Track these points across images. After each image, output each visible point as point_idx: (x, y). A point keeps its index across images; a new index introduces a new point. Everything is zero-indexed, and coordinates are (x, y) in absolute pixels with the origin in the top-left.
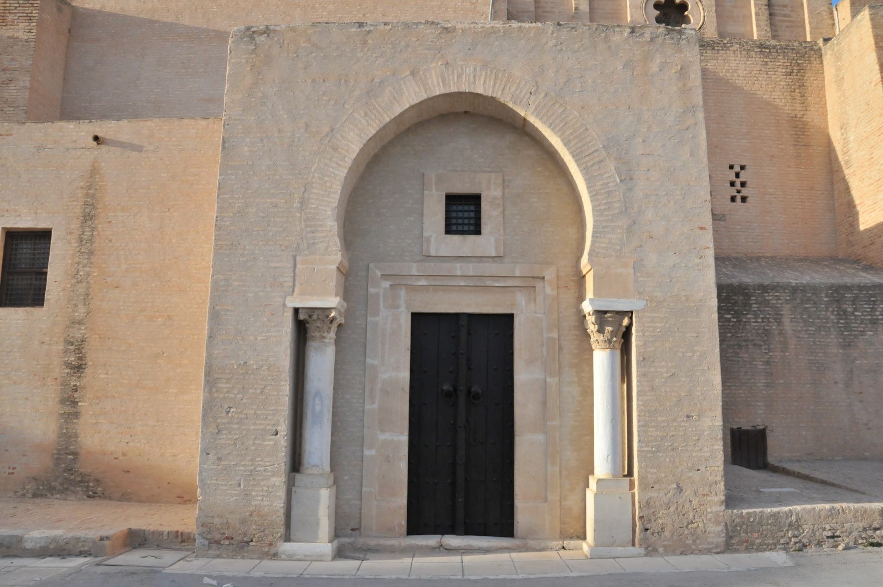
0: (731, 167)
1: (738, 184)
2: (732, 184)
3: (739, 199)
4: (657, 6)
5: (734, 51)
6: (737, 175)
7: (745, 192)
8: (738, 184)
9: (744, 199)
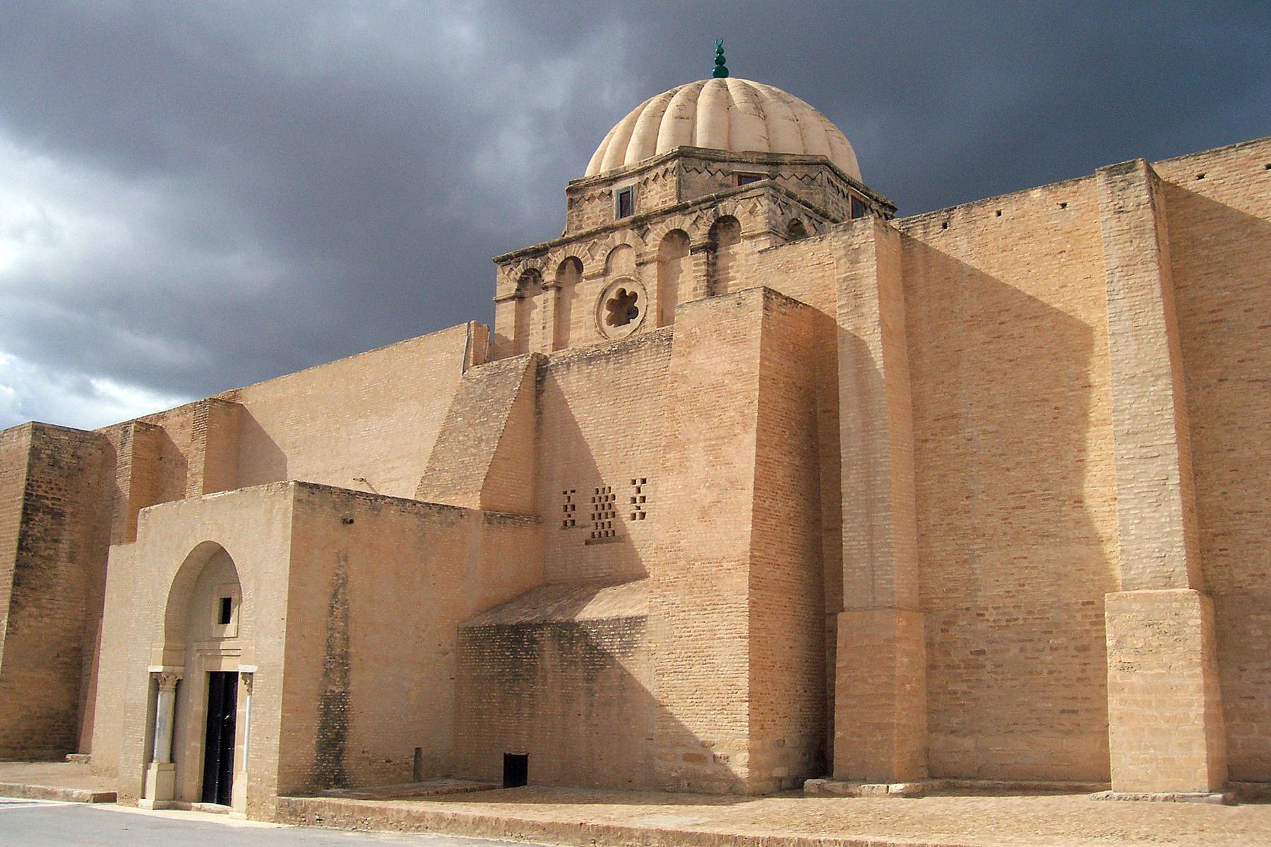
0: (634, 482)
2: (634, 500)
6: (639, 491)
9: (643, 515)
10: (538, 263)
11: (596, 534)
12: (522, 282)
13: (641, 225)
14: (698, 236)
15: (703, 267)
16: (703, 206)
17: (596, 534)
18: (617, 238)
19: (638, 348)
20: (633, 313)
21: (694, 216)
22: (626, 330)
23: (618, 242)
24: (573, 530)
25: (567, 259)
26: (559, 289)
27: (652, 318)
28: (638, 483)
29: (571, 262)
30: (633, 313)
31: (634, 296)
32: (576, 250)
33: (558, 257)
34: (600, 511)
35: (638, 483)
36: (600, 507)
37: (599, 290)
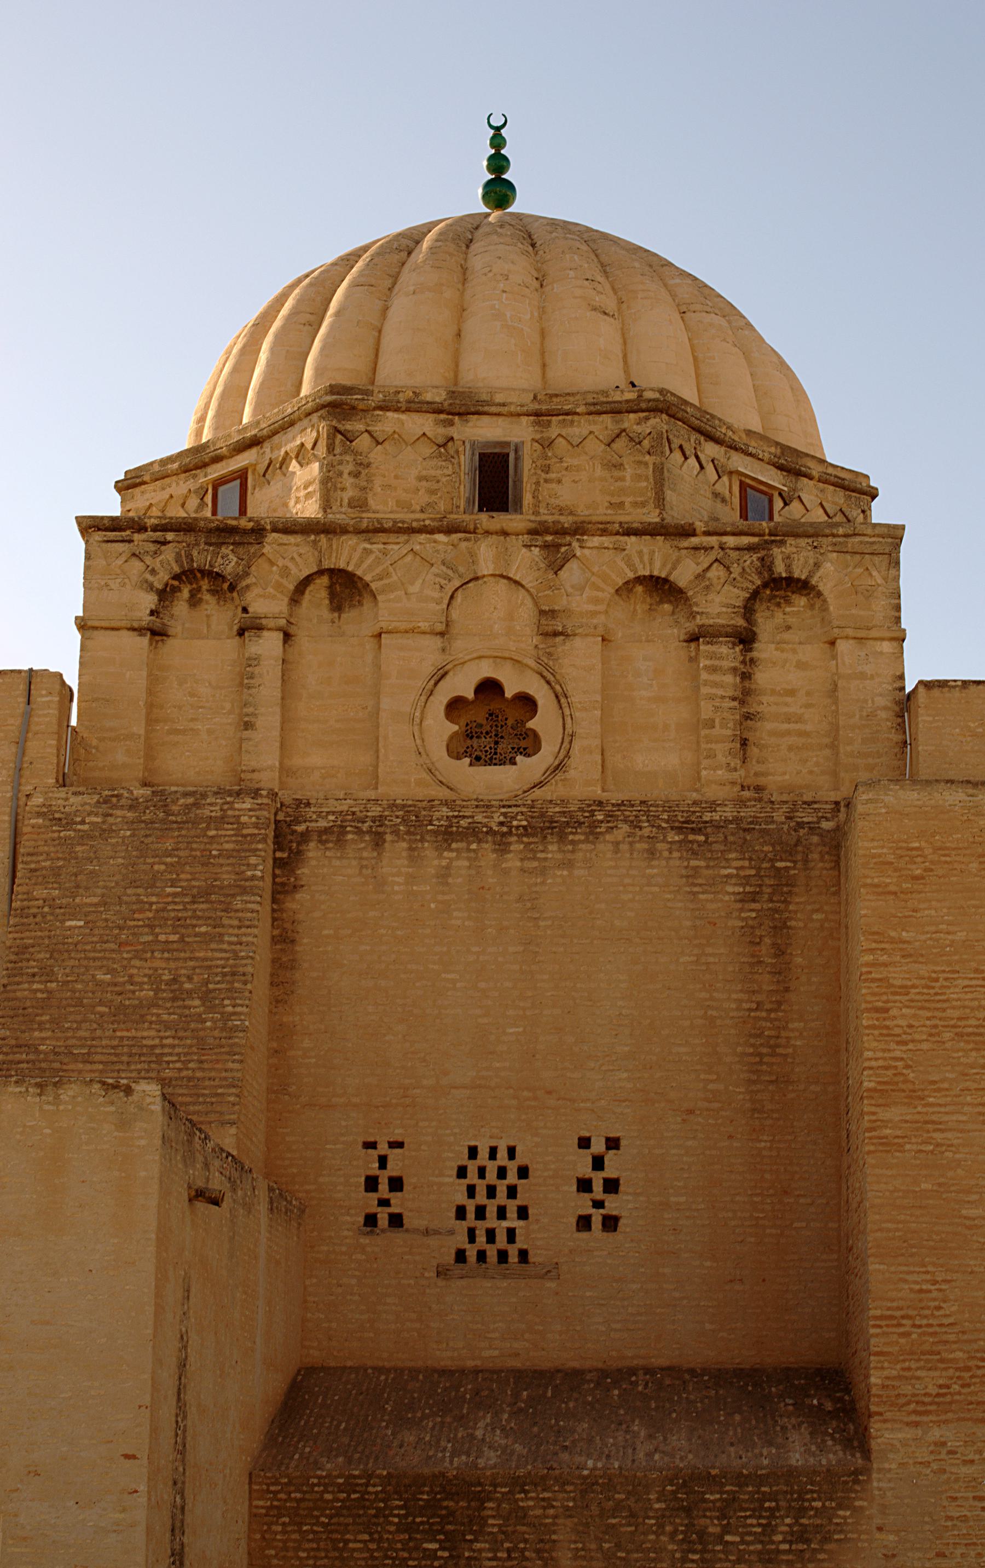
0: (584, 1143)
1: (598, 1186)
2: (584, 1185)
3: (597, 1222)
6: (598, 1163)
7: (613, 1205)
8: (598, 1186)
9: (611, 1223)
10: (228, 561)
11: (472, 1254)
13: (556, 540)
14: (719, 604)
15: (729, 679)
16: (731, 541)
17: (472, 1254)
18: (486, 555)
19: (593, 834)
20: (529, 744)
21: (705, 560)
22: (502, 780)
24: (398, 1237)
25: (321, 572)
26: (287, 636)
28: (598, 1146)
29: (324, 580)
30: (529, 744)
32: (347, 554)
34: (481, 1198)
35: (598, 1146)
37: (428, 668)
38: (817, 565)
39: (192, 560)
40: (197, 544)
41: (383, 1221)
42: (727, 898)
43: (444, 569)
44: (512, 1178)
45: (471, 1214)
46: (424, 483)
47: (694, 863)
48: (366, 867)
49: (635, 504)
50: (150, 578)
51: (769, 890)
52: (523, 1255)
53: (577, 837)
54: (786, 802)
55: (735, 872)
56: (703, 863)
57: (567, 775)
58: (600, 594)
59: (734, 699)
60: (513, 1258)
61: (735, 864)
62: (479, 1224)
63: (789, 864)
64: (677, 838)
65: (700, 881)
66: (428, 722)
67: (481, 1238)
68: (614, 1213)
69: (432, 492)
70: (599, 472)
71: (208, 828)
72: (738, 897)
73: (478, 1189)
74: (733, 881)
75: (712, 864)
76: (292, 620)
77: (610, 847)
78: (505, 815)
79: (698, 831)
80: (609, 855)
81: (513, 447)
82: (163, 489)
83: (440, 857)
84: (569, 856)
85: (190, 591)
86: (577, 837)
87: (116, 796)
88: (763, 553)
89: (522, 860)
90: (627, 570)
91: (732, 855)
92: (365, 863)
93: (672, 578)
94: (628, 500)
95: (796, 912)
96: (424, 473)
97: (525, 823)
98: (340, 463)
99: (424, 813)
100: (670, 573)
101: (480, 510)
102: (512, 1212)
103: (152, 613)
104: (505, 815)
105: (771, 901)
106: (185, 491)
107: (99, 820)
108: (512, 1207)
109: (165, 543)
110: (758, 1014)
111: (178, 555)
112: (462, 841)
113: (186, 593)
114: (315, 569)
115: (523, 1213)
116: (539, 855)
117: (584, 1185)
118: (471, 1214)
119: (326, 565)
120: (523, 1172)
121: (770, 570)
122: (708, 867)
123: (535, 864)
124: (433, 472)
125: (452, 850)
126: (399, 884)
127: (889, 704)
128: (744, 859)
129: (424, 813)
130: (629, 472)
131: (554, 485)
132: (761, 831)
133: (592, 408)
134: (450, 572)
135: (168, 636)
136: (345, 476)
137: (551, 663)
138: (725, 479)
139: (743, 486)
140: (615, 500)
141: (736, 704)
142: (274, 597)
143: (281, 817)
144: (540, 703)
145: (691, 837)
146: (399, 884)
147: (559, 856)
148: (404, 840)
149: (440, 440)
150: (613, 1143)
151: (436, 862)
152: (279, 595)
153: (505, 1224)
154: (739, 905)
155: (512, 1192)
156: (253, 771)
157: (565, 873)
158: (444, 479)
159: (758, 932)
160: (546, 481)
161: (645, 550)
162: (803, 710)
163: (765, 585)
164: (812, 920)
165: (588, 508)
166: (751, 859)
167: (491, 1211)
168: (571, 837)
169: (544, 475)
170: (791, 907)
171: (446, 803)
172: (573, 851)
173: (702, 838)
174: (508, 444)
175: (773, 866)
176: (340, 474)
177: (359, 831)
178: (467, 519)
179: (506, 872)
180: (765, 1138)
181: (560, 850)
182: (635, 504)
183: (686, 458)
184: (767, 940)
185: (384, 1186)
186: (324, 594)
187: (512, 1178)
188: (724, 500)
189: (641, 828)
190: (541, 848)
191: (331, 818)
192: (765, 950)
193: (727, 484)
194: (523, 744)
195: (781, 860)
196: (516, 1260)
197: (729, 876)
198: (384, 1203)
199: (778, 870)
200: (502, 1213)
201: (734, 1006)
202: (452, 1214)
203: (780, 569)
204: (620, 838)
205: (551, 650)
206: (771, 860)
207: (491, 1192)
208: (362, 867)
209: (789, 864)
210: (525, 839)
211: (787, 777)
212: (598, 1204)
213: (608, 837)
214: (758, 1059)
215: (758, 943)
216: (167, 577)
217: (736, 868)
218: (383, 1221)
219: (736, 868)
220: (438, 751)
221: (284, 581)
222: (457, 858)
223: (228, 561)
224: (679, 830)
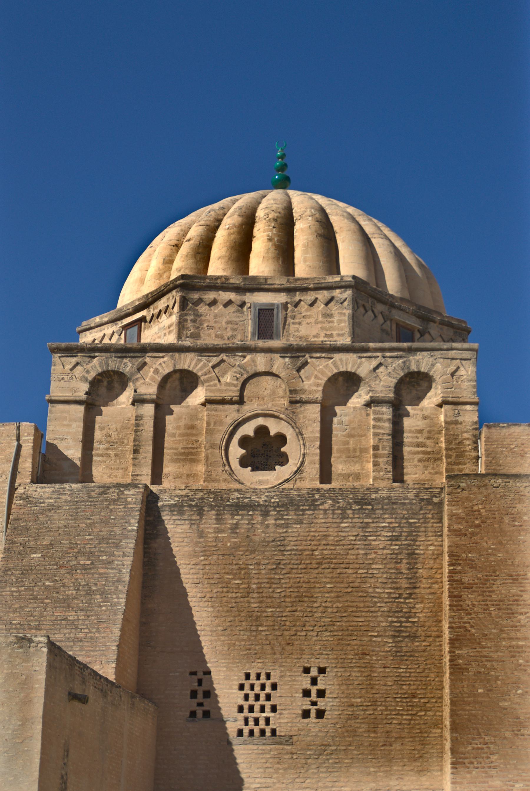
0: (307, 670)
2: (307, 693)
3: (313, 714)
4: (244, 442)
5: (325, 510)
6: (314, 681)
7: (322, 704)
9: (320, 714)
10: (127, 366)
11: (246, 732)
12: (95, 383)
17: (246, 732)
20: (283, 460)
21: (374, 363)
23: (261, 368)
25: (175, 371)
27: (313, 469)
28: (314, 672)
29: (178, 375)
30: (283, 460)
31: (282, 439)
33: (164, 365)
36: (252, 698)
37: (229, 420)
38: (433, 365)
39: (108, 366)
40: (111, 357)
41: (199, 713)
42: (383, 539)
43: (239, 369)
44: (268, 690)
45: (246, 710)
46: (230, 325)
47: (366, 520)
48: (194, 524)
49: (338, 335)
50: (86, 375)
51: (405, 534)
52: (274, 732)
53: (305, 508)
54: (415, 489)
55: (387, 525)
56: (370, 520)
57: (302, 476)
58: (320, 381)
59: (389, 435)
60: (268, 733)
61: (388, 521)
62: (250, 715)
63: (415, 520)
64: (357, 507)
65: (369, 530)
66: (231, 449)
67: (251, 723)
68: (323, 708)
69: (234, 330)
70: (320, 318)
71: (110, 504)
72: (389, 538)
73: (250, 696)
74: (387, 529)
75: (375, 521)
76: (160, 396)
77: (322, 512)
78: (267, 496)
79: (366, 504)
80: (321, 516)
81: (276, 307)
82: (101, 331)
83: (233, 518)
84: (300, 517)
85: (108, 382)
86: (305, 508)
87: (63, 488)
88: (405, 359)
89: (276, 520)
90: (334, 369)
91: (386, 516)
92: (193, 522)
93: (357, 373)
94: (335, 333)
95: (419, 546)
96: (230, 319)
97: (277, 500)
98: (186, 315)
99: (225, 496)
100: (357, 370)
101: (258, 339)
102: (268, 709)
103: (87, 393)
104: (267, 496)
105: (406, 540)
106: (111, 332)
107: (52, 501)
108: (268, 705)
109: (94, 357)
110: (399, 600)
111: (101, 363)
112: (244, 510)
113: (105, 383)
114: (172, 370)
115: (274, 709)
116: (285, 517)
117: (307, 693)
118: (246, 710)
119: (178, 367)
120: (274, 687)
121: (408, 368)
122: (373, 522)
123: (283, 522)
124: (234, 319)
125: (238, 515)
126: (211, 533)
127: (470, 437)
128: (392, 518)
129: (225, 496)
130: (336, 319)
131: (297, 326)
132: (401, 503)
133: (317, 286)
134: (242, 371)
135: (95, 405)
136: (189, 321)
137: (294, 417)
138: (388, 322)
139: (397, 325)
140: (328, 333)
141: (390, 437)
142: (150, 384)
143: (150, 498)
144: (288, 438)
145: (365, 507)
146: (211, 533)
147: (295, 517)
148: (214, 510)
149: (239, 303)
150: (322, 671)
151: (231, 522)
152: (153, 383)
153: (264, 715)
154: (389, 542)
155: (268, 697)
156: (138, 475)
157: (299, 526)
158: (240, 323)
159: (399, 557)
160: (293, 323)
161: (344, 359)
162: (425, 440)
163: (406, 376)
164: (428, 550)
165: (315, 336)
166: (396, 518)
167: (257, 708)
168: (301, 508)
169: (292, 321)
170: (418, 543)
171: (237, 490)
172: (303, 515)
173: (370, 507)
174: (273, 304)
175: (408, 522)
176: (186, 320)
177: (190, 506)
178: (250, 342)
179: (267, 526)
180: (403, 667)
181: (295, 515)
182: (338, 335)
183: (366, 311)
184: (404, 561)
185: (200, 695)
186: (177, 383)
187: (268, 690)
188: (387, 333)
189: (338, 503)
190: (286, 513)
191: (176, 499)
192: (403, 567)
193: (389, 325)
194: (281, 460)
195: (412, 518)
196: (270, 734)
197: (384, 527)
198: (200, 705)
199: (411, 523)
200: (262, 709)
201: (386, 596)
202: (236, 709)
203: (414, 368)
204: (327, 507)
205: (294, 410)
206: (406, 518)
207: (257, 698)
208: (192, 524)
209: (415, 520)
210: (278, 509)
211: (417, 476)
212: (314, 704)
213: (321, 507)
214: (399, 624)
215: (400, 563)
216: (95, 375)
217: (388, 523)
218: (199, 713)
219: (388, 523)
220: (235, 463)
221: (156, 376)
222: (242, 519)
223: (127, 366)
224: (357, 503)
